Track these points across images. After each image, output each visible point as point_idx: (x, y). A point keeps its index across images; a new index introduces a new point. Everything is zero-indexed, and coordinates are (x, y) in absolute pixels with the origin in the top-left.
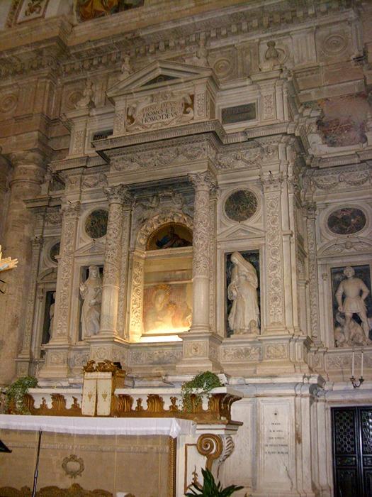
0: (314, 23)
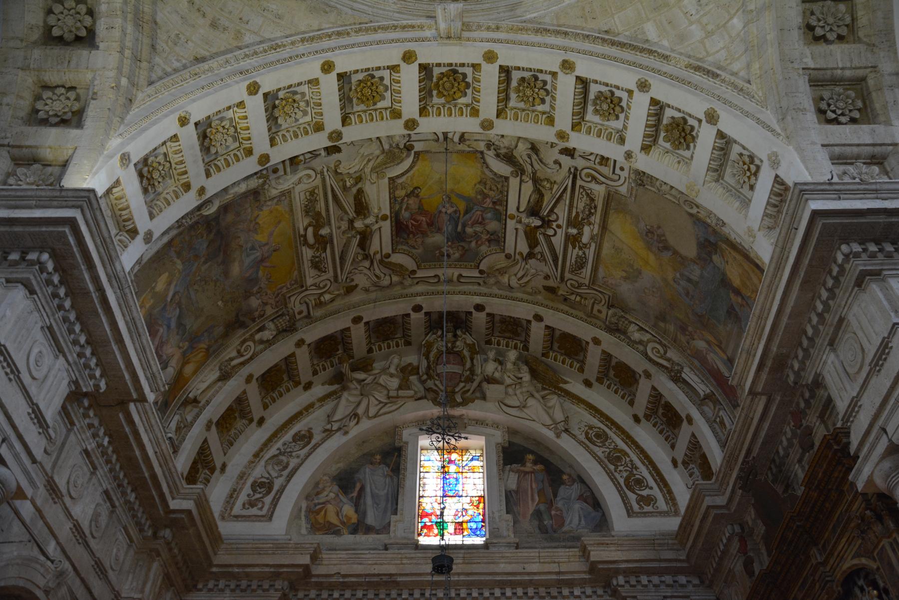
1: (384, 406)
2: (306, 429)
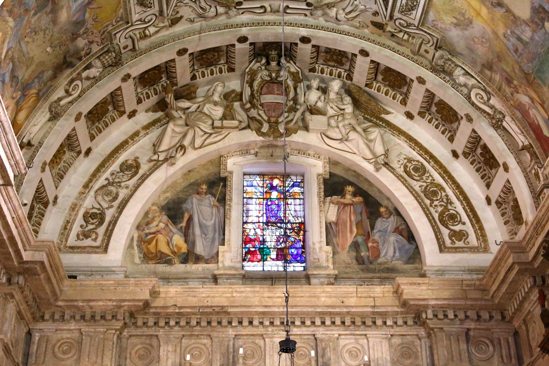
0: (392, 331)
1: (209, 136)
2: (133, 158)
